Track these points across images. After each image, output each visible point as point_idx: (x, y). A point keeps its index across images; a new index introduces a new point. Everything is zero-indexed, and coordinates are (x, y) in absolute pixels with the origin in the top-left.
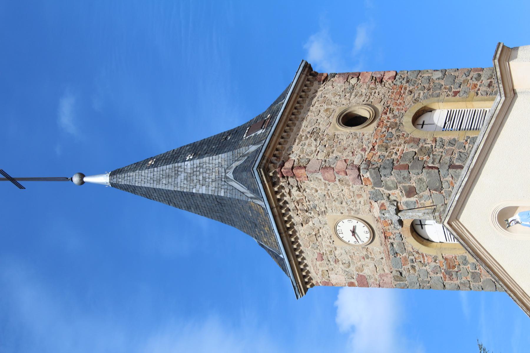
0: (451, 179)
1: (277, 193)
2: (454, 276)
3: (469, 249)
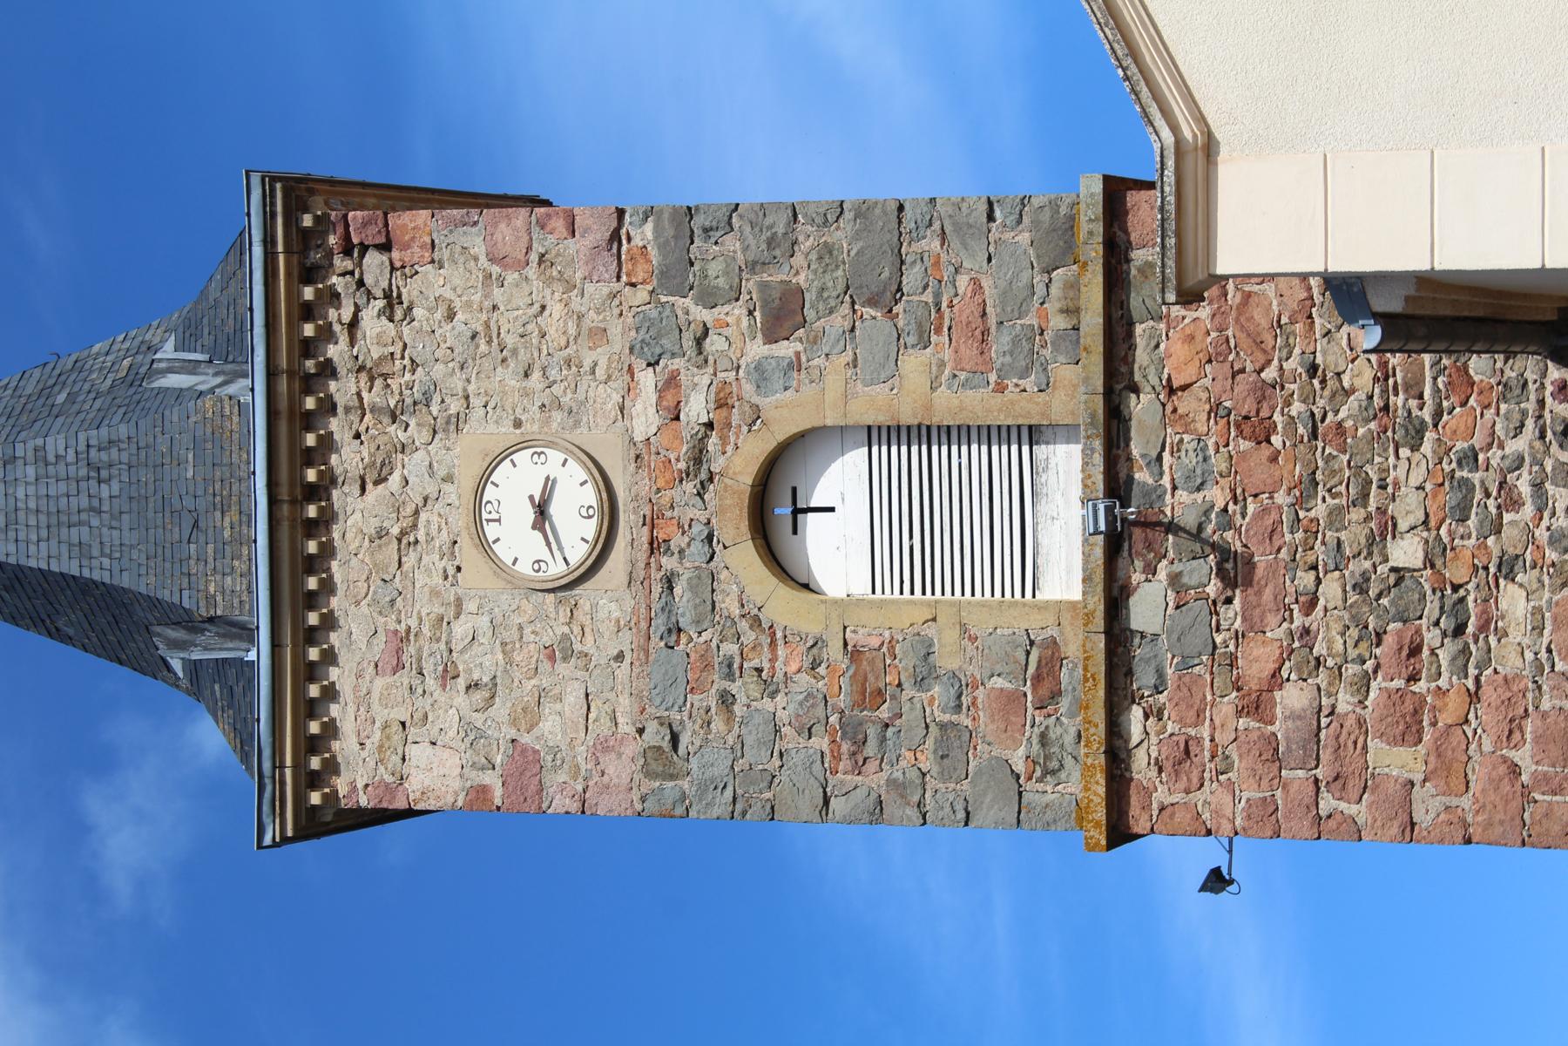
0: (937, 243)
1: (308, 312)
2: (871, 749)
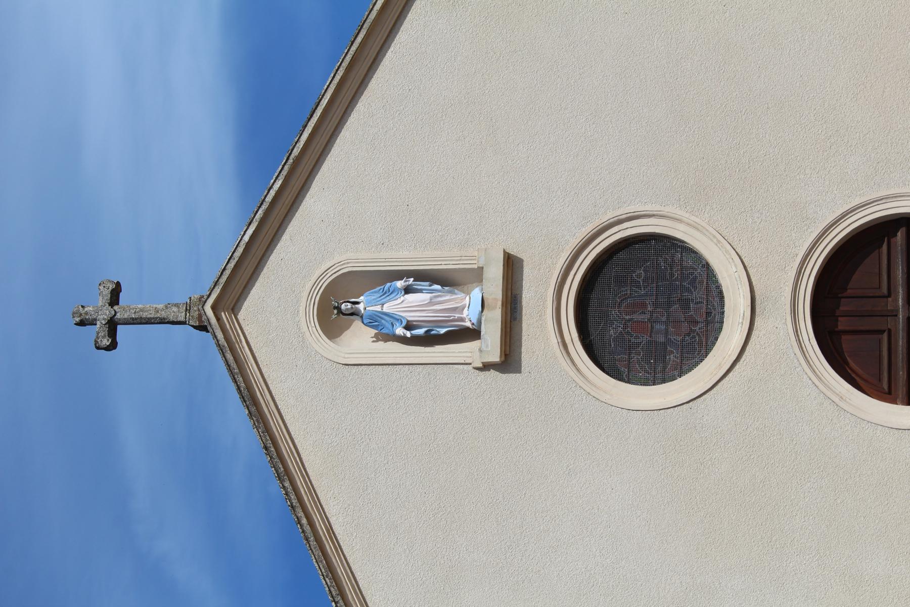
3: (240, 379)
